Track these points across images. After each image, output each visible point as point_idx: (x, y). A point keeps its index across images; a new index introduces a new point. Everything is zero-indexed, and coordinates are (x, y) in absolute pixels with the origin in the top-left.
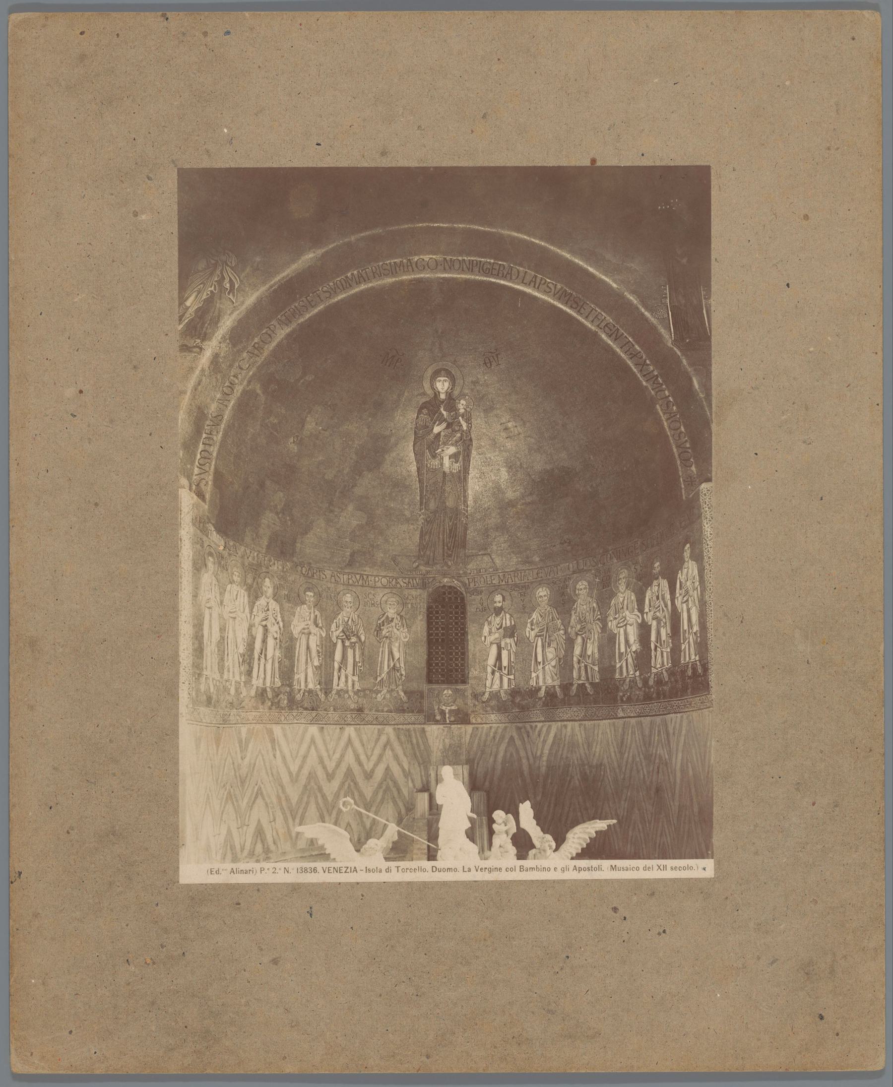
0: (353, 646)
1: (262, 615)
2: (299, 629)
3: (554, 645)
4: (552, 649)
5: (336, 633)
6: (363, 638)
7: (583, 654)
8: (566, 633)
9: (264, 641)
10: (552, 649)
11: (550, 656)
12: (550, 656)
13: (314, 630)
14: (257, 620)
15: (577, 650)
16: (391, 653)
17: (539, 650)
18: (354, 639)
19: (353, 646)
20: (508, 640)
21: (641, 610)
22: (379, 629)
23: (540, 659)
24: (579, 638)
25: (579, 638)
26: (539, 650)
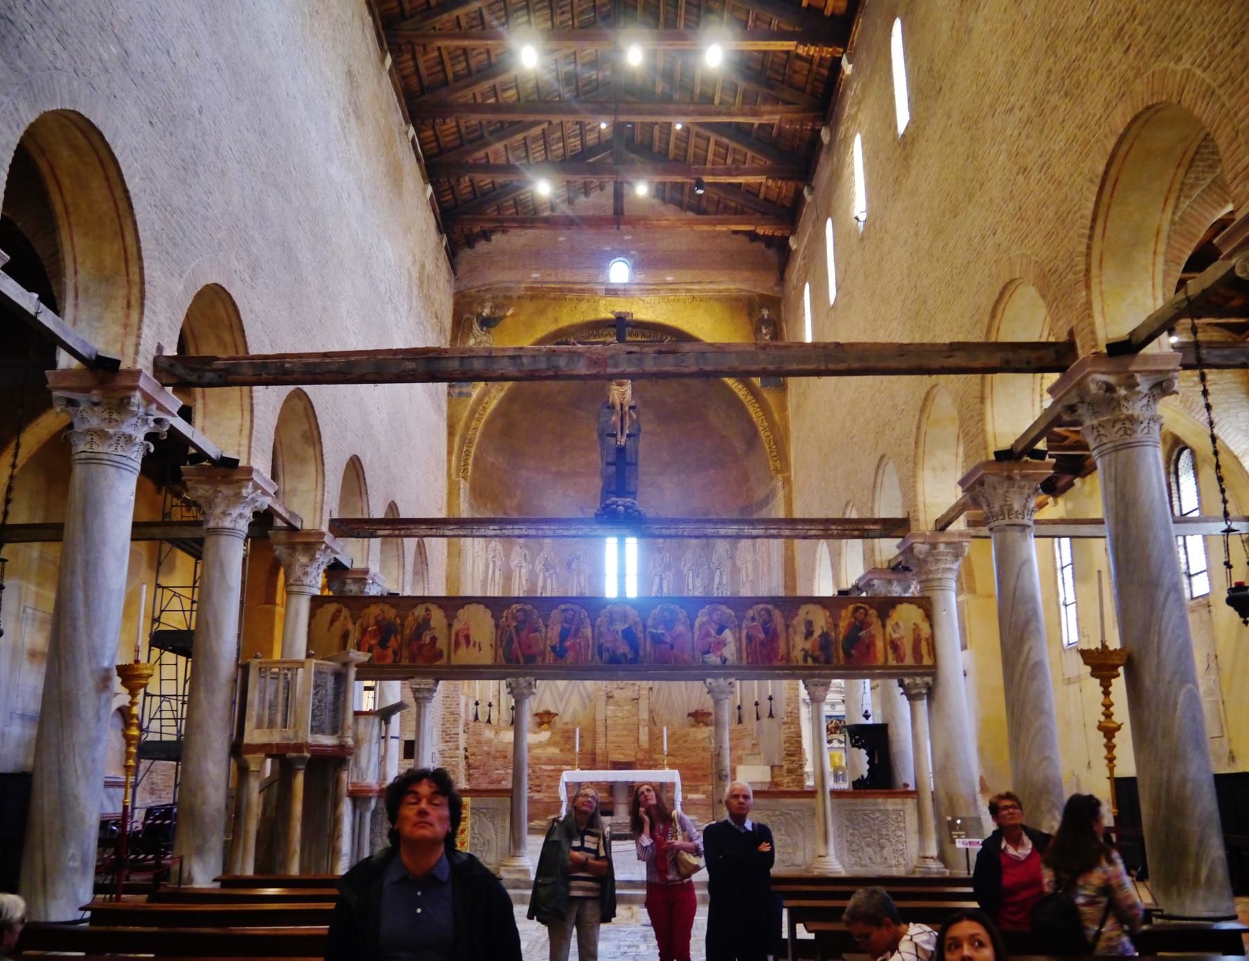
0: (551, 575)
1: (492, 554)
2: (515, 563)
3: (701, 576)
4: (699, 580)
5: (539, 566)
6: (558, 571)
7: (720, 583)
8: (709, 568)
9: (494, 572)
10: (699, 580)
11: (698, 585)
12: (698, 585)
13: (524, 564)
14: (490, 557)
15: (717, 580)
16: (579, 582)
17: (690, 580)
18: (551, 571)
19: (551, 575)
20: (668, 573)
21: (755, 552)
22: (569, 564)
23: (691, 587)
24: (718, 572)
25: (718, 572)
26: (690, 580)
